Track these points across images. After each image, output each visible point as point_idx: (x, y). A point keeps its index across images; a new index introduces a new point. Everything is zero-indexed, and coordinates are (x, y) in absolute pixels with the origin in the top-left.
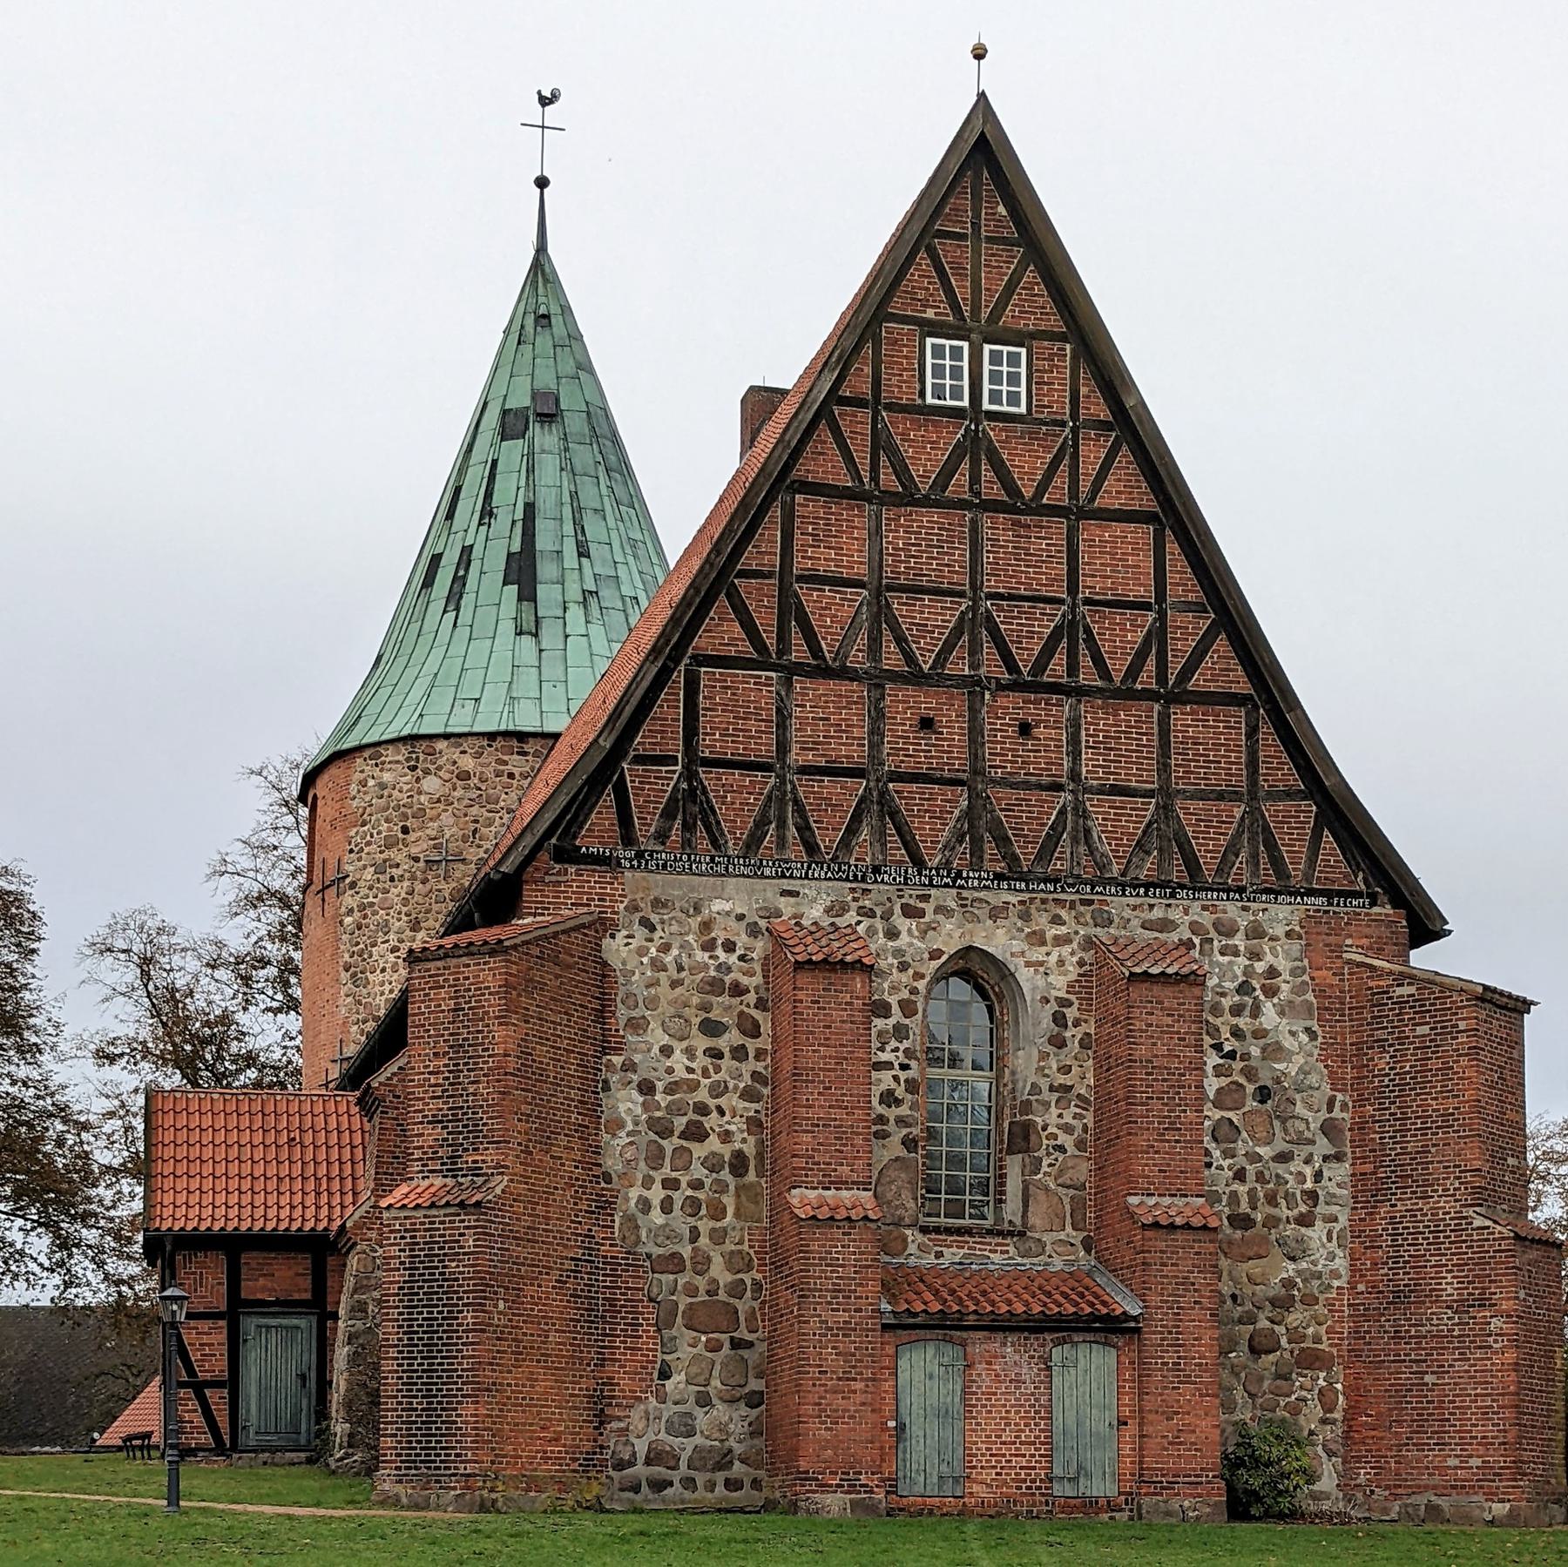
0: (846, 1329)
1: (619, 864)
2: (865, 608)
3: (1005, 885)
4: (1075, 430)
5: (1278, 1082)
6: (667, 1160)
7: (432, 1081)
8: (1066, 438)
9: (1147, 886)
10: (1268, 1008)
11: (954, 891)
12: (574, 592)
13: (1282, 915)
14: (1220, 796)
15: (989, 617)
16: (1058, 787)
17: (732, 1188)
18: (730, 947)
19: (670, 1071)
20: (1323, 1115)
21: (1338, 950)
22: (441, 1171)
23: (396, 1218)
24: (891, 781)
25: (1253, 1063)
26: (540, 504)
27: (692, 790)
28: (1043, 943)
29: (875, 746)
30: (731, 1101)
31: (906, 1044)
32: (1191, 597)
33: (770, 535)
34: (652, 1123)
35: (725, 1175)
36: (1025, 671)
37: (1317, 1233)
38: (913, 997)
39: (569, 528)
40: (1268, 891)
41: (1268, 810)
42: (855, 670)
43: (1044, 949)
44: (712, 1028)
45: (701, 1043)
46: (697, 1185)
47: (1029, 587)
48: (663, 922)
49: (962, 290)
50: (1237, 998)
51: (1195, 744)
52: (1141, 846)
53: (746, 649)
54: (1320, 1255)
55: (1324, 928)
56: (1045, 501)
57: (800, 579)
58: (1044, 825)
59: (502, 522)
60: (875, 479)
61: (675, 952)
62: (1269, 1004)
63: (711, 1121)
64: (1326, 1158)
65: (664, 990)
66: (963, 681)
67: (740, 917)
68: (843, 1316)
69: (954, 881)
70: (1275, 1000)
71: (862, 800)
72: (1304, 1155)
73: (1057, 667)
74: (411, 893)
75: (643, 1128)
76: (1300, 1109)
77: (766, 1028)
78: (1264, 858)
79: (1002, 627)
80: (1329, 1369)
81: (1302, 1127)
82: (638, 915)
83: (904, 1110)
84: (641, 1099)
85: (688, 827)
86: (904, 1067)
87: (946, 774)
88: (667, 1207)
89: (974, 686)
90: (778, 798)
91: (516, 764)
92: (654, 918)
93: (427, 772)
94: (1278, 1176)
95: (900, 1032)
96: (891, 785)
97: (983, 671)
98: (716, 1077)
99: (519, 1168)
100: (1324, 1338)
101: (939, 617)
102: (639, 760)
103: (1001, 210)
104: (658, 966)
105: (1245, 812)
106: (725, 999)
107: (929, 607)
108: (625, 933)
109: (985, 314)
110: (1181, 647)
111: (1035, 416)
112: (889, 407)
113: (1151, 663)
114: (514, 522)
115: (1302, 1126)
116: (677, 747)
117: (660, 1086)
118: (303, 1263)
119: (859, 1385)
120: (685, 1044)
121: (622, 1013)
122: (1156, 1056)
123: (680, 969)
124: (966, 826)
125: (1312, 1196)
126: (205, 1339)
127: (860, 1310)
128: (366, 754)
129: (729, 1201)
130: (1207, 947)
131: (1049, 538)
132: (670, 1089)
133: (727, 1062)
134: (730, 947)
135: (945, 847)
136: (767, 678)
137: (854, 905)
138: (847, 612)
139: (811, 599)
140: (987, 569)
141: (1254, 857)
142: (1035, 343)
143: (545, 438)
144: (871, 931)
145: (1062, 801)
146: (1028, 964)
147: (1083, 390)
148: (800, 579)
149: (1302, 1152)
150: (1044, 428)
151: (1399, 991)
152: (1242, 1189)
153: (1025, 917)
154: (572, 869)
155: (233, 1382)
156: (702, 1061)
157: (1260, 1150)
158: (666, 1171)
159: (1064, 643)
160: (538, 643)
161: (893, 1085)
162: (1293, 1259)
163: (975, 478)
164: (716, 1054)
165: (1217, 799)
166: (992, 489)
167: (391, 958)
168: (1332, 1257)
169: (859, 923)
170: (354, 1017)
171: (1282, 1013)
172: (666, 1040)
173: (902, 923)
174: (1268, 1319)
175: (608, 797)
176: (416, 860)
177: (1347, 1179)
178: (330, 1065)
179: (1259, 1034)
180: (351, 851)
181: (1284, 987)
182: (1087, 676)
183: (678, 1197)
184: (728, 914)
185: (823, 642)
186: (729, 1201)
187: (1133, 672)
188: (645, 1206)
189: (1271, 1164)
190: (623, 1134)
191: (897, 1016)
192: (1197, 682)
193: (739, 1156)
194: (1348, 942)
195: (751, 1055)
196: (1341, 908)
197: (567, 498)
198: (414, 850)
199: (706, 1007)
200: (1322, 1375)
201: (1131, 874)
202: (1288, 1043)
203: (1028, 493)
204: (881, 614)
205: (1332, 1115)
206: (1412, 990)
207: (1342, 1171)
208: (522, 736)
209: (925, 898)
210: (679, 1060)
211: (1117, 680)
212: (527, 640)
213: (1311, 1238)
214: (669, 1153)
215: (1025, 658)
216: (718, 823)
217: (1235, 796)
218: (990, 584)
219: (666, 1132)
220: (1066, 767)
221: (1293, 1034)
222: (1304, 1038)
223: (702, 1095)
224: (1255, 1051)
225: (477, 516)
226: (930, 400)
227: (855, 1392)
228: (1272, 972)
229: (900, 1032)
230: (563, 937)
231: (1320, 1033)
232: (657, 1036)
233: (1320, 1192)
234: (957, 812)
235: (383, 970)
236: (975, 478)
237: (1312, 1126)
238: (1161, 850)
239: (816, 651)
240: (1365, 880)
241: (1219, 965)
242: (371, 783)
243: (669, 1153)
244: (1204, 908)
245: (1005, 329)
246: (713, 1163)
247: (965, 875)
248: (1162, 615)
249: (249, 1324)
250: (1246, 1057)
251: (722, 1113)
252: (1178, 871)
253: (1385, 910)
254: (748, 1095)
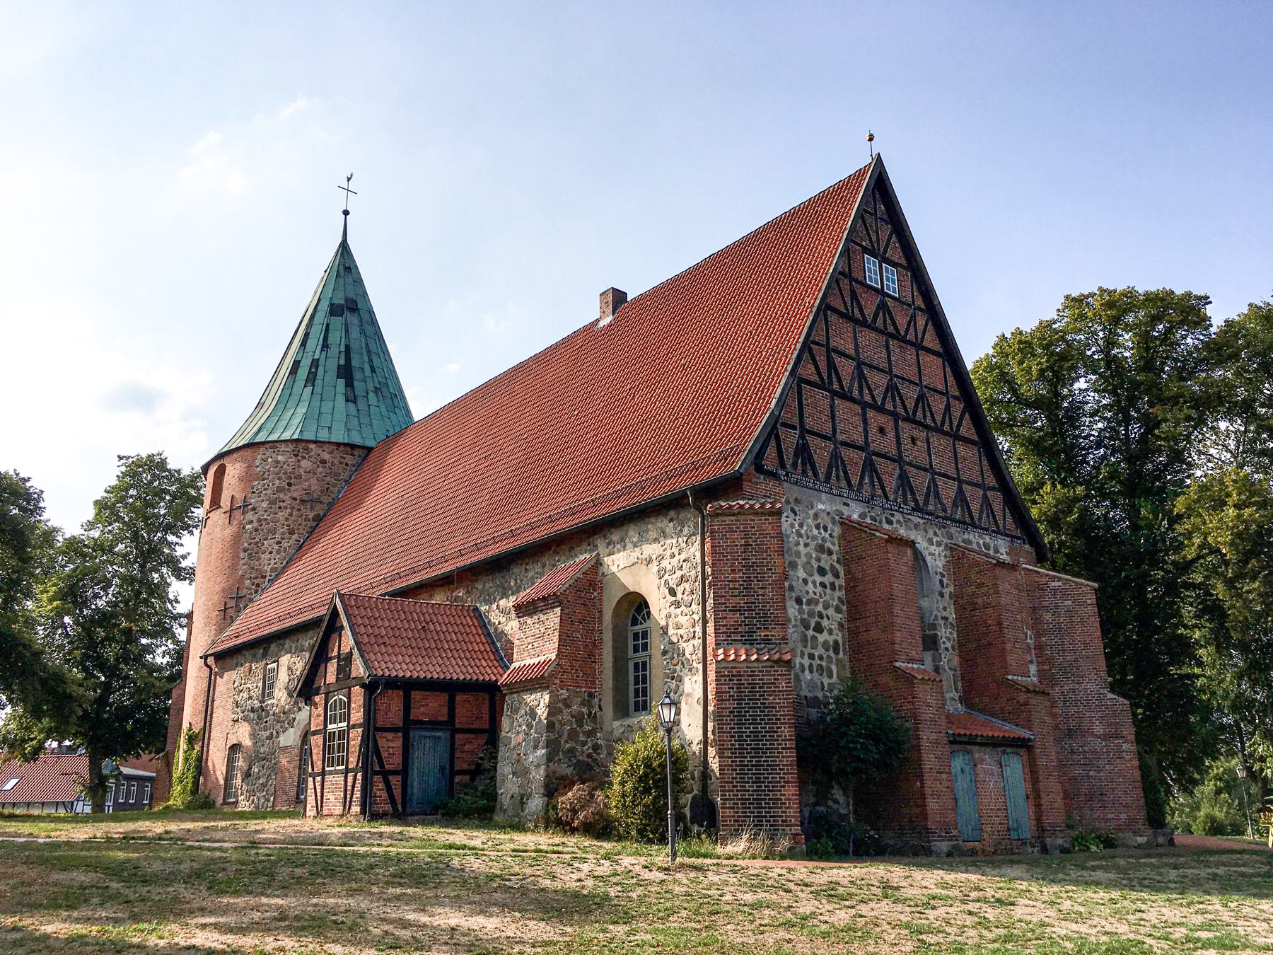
7: (731, 586)
12: (371, 387)
17: (834, 660)
18: (825, 529)
19: (807, 592)
22: (742, 640)
23: (725, 668)
26: (352, 345)
29: (866, 437)
30: (831, 612)
34: (803, 621)
35: (831, 653)
39: (366, 359)
44: (822, 571)
45: (818, 579)
46: (821, 658)
48: (799, 511)
53: (815, 378)
59: (334, 350)
61: (805, 528)
63: (825, 623)
65: (801, 548)
67: (828, 514)
74: (291, 515)
75: (799, 623)
77: (842, 574)
84: (797, 607)
85: (804, 464)
89: (895, 415)
90: (835, 456)
91: (349, 459)
93: (304, 458)
97: (898, 409)
98: (825, 598)
104: (800, 536)
106: (824, 556)
114: (340, 352)
116: (796, 421)
117: (804, 600)
118: (444, 697)
123: (808, 538)
126: (391, 745)
128: (267, 446)
129: (834, 667)
133: (828, 591)
134: (825, 529)
143: (353, 319)
151: (1053, 584)
155: (404, 772)
156: (819, 589)
158: (808, 650)
160: (357, 406)
164: (823, 585)
167: (276, 547)
170: (248, 576)
172: (805, 575)
175: (773, 442)
176: (295, 499)
178: (228, 600)
180: (253, 492)
182: (929, 421)
184: (824, 511)
186: (834, 667)
193: (836, 642)
195: (837, 588)
197: (364, 346)
198: (295, 495)
199: (818, 560)
206: (1060, 584)
208: (353, 447)
209: (893, 515)
212: (351, 405)
219: (807, 627)
223: (820, 608)
225: (319, 347)
232: (801, 574)
235: (271, 553)
242: (270, 460)
246: (826, 646)
249: (415, 735)
251: (829, 619)
254: (838, 610)
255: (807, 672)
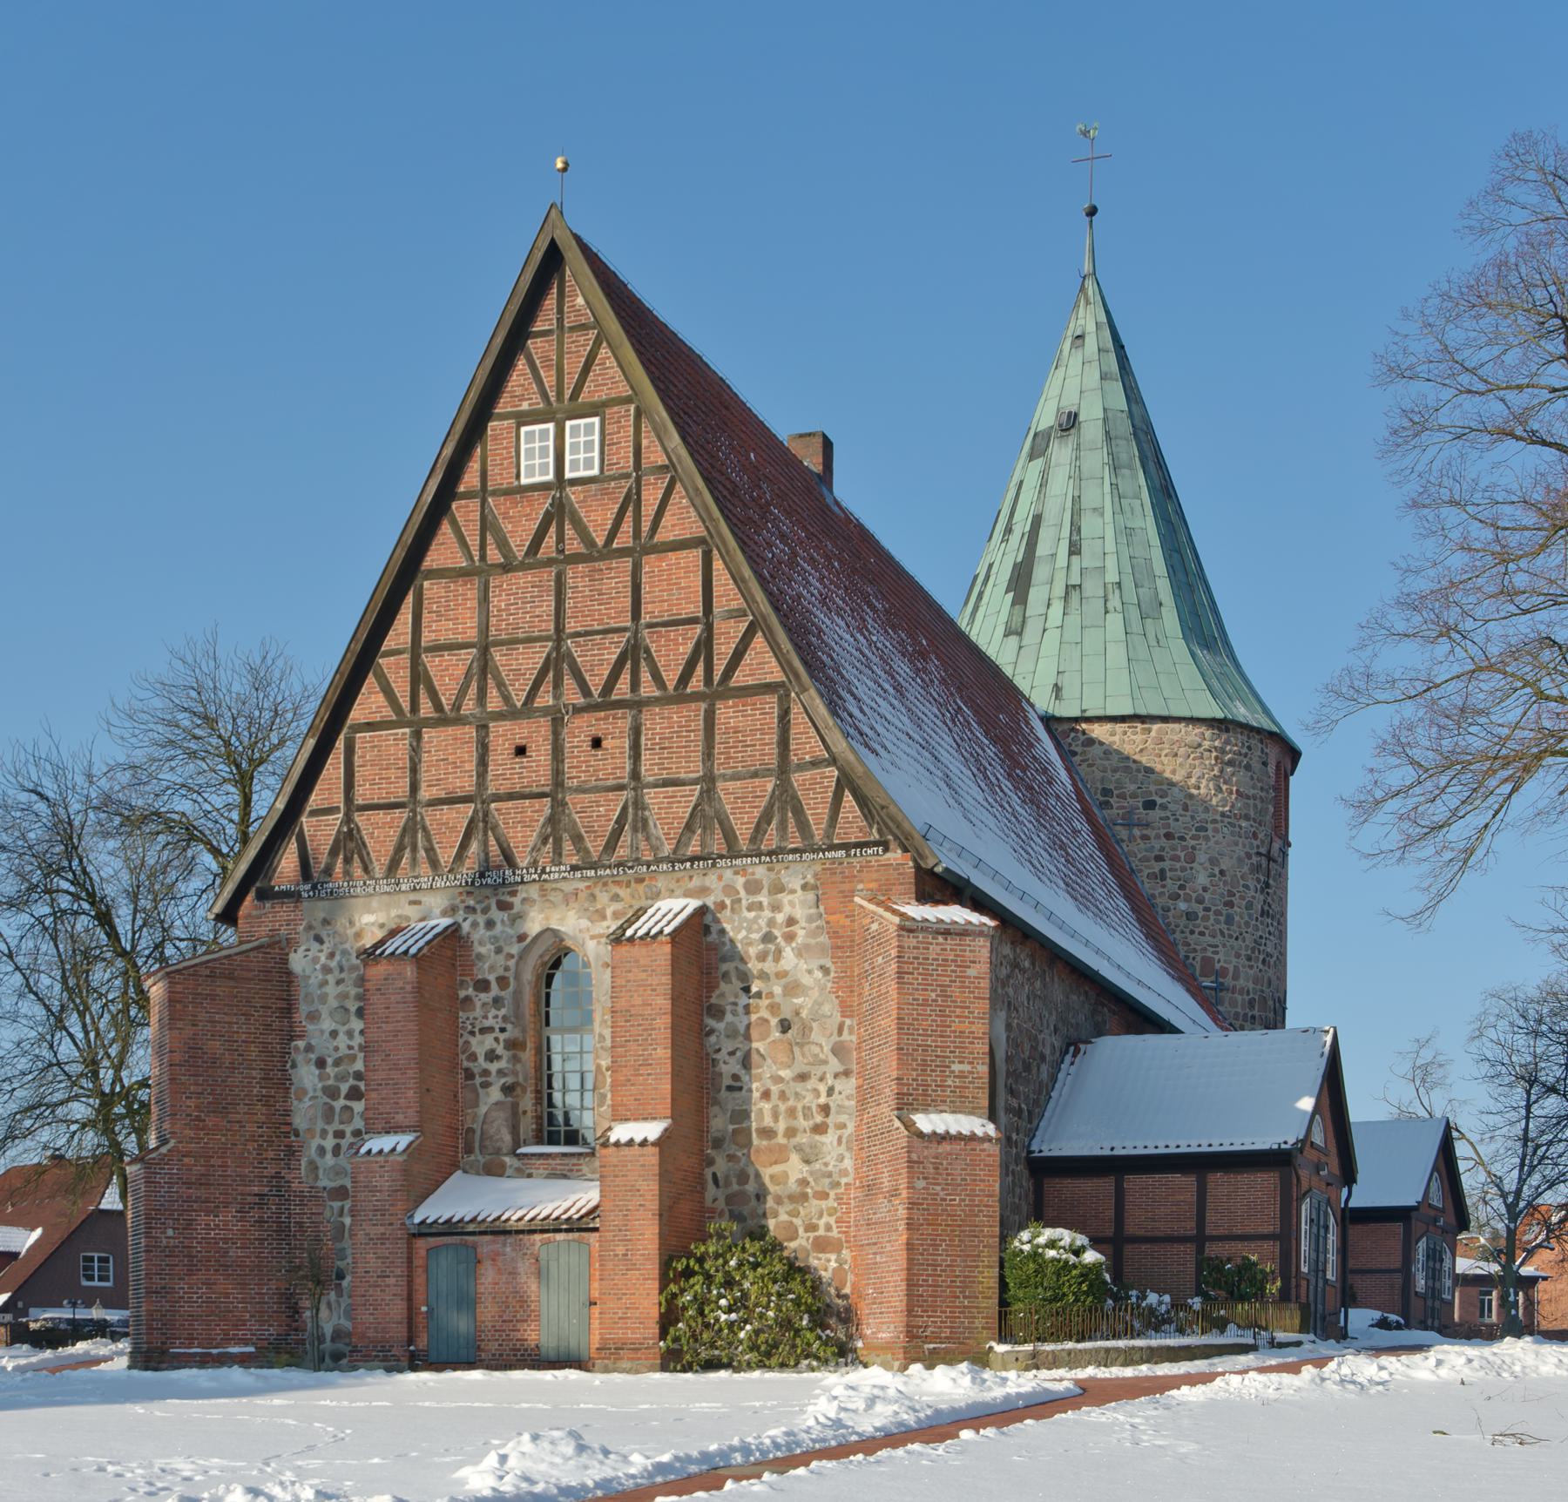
0: (383, 1238)
1: (300, 896)
2: (475, 664)
3: (578, 874)
4: (638, 480)
5: (797, 1014)
6: (337, 1117)
8: (630, 489)
9: (693, 859)
10: (788, 953)
11: (537, 886)
13: (796, 874)
14: (755, 775)
15: (570, 654)
16: (621, 788)
19: (336, 1049)
20: (835, 1038)
21: (852, 893)
24: (493, 801)
25: (777, 1000)
27: (350, 831)
28: (604, 918)
31: (503, 1011)
32: (734, 605)
33: (405, 617)
34: (325, 1090)
36: (596, 694)
37: (829, 1139)
38: (507, 974)
40: (794, 851)
41: (797, 781)
42: (467, 716)
43: (605, 924)
47: (600, 621)
48: (329, 935)
49: (549, 379)
50: (761, 947)
51: (735, 732)
52: (689, 827)
53: (388, 713)
54: (831, 1159)
55: (838, 878)
56: (615, 546)
57: (429, 650)
58: (610, 820)
60: (483, 557)
61: (337, 958)
62: (788, 949)
64: (836, 1076)
66: (545, 711)
68: (382, 1229)
69: (540, 876)
70: (794, 945)
71: (472, 821)
72: (819, 1074)
73: (623, 687)
75: (319, 1093)
76: (815, 1036)
78: (791, 822)
79: (579, 660)
80: (839, 1252)
81: (816, 1050)
82: (312, 933)
83: (503, 1064)
84: (317, 1072)
85: (348, 861)
86: (503, 1030)
87: (535, 790)
88: (337, 1150)
90: (411, 829)
92: (324, 934)
94: (797, 1094)
95: (497, 1001)
96: (493, 805)
99: (191, 1133)
100: (834, 1226)
101: (535, 657)
102: (314, 813)
103: (580, 301)
105: (776, 785)
107: (523, 653)
108: (303, 948)
109: (568, 393)
110: (723, 650)
111: (607, 473)
112: (494, 493)
113: (700, 669)
115: (816, 1050)
116: (339, 799)
117: (330, 1061)
119: (392, 1281)
120: (346, 1028)
121: (303, 1009)
122: (634, 1006)
123: (342, 970)
124: (549, 830)
125: (825, 1110)
127: (391, 1224)
130: (736, 906)
131: (617, 576)
132: (337, 1063)
135: (533, 850)
136: (404, 734)
137: (462, 906)
138: (460, 671)
139: (431, 662)
140: (569, 613)
141: (783, 826)
142: (608, 411)
144: (475, 925)
145: (624, 798)
146: (592, 937)
147: (644, 442)
148: (429, 650)
149: (817, 1071)
150: (613, 484)
152: (766, 1106)
153: (593, 897)
154: (268, 905)
157: (782, 1073)
158: (336, 1126)
159: (628, 665)
161: (495, 1045)
162: (807, 1162)
163: (561, 538)
165: (751, 777)
166: (574, 545)
168: (841, 1158)
169: (465, 920)
171: (799, 953)
173: (496, 914)
174: (787, 1213)
177: (854, 1092)
179: (781, 975)
181: (801, 933)
183: (344, 1143)
184: (373, 924)
185: (443, 699)
187: (685, 678)
188: (322, 1151)
189: (792, 1083)
190: (306, 1099)
191: (495, 990)
192: (740, 678)
194: (860, 886)
196: (857, 859)
200: (833, 1257)
201: (681, 852)
202: (806, 980)
203: (600, 542)
204: (484, 666)
205: (842, 1038)
207: (848, 1086)
210: (342, 1041)
211: (671, 686)
213: (823, 1144)
214: (338, 1110)
215: (596, 683)
216: (368, 854)
217: (766, 773)
218: (571, 626)
219: (332, 1093)
220: (628, 769)
221: (810, 972)
222: (819, 974)
224: (777, 990)
226: (524, 481)
227: (388, 1286)
228: (791, 921)
229: (497, 1001)
230: (238, 958)
231: (833, 968)
232: (327, 1024)
233: (831, 1104)
234: (542, 820)
236: (561, 538)
237: (825, 1049)
238: (705, 828)
239: (438, 706)
240: (879, 831)
241: (746, 919)
243: (338, 1110)
244: (736, 873)
245: (584, 404)
247: (548, 870)
248: (709, 628)
250: (771, 995)
252: (717, 844)
253: (895, 855)
255: (329, 1156)
